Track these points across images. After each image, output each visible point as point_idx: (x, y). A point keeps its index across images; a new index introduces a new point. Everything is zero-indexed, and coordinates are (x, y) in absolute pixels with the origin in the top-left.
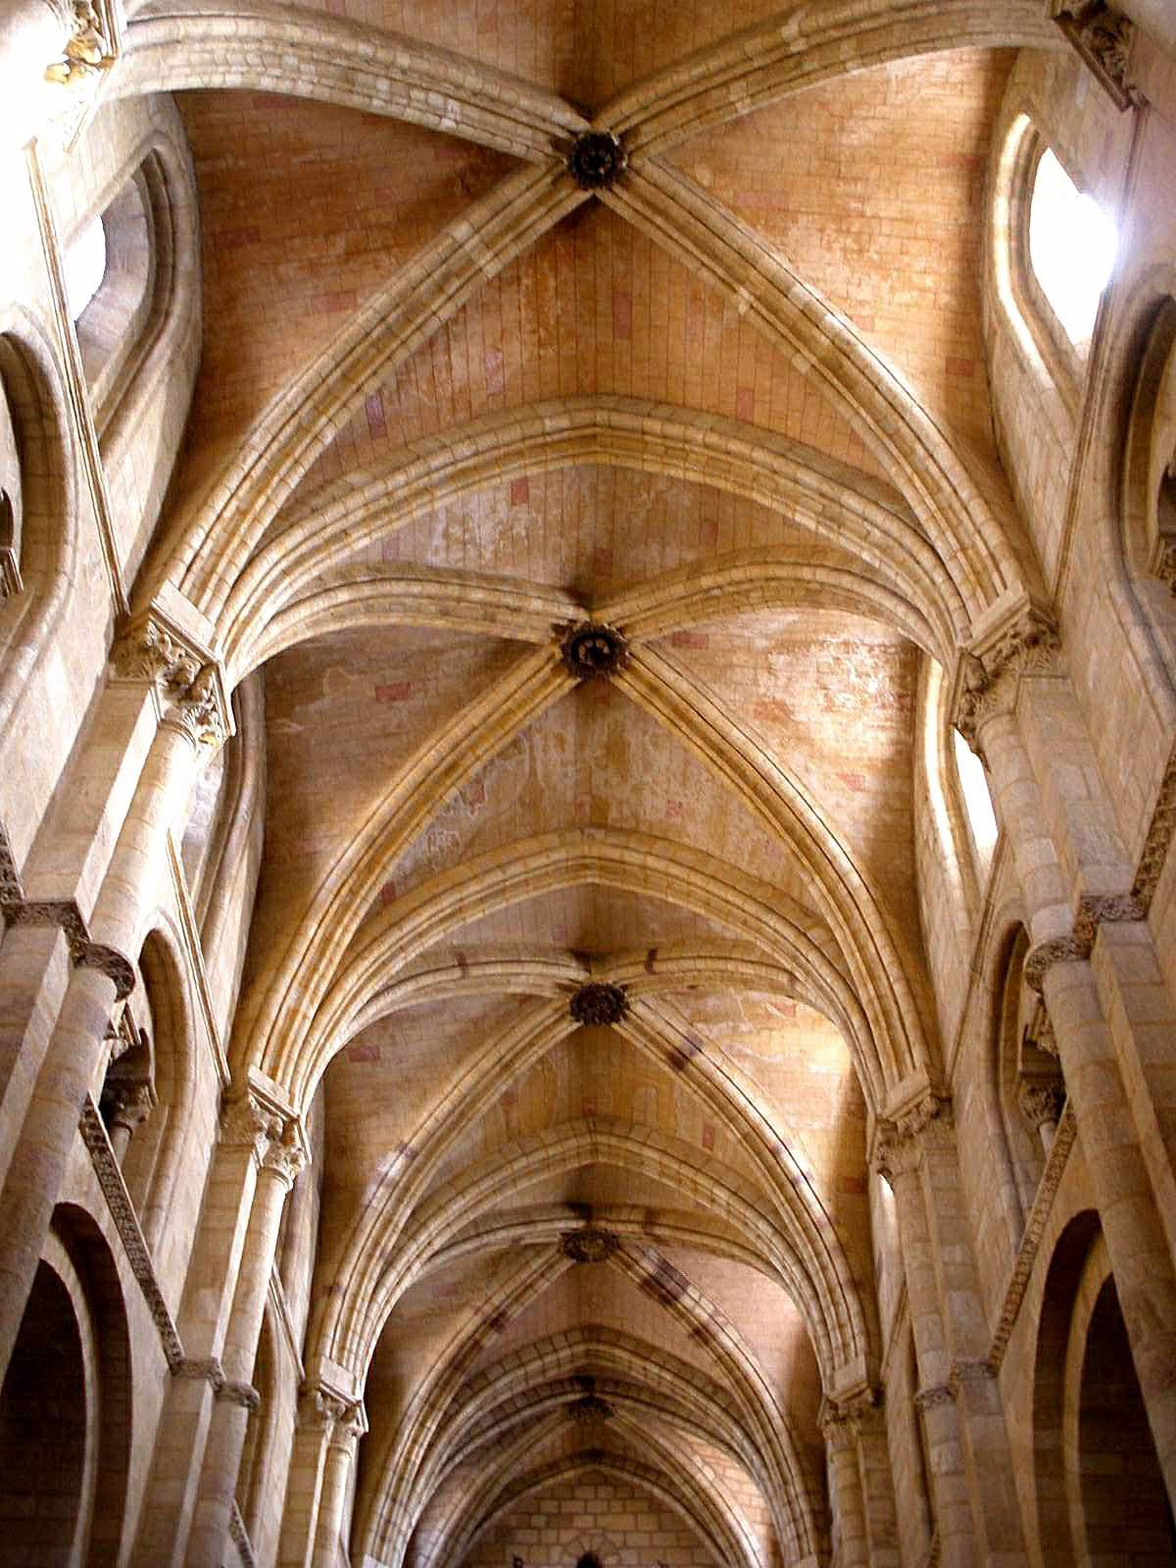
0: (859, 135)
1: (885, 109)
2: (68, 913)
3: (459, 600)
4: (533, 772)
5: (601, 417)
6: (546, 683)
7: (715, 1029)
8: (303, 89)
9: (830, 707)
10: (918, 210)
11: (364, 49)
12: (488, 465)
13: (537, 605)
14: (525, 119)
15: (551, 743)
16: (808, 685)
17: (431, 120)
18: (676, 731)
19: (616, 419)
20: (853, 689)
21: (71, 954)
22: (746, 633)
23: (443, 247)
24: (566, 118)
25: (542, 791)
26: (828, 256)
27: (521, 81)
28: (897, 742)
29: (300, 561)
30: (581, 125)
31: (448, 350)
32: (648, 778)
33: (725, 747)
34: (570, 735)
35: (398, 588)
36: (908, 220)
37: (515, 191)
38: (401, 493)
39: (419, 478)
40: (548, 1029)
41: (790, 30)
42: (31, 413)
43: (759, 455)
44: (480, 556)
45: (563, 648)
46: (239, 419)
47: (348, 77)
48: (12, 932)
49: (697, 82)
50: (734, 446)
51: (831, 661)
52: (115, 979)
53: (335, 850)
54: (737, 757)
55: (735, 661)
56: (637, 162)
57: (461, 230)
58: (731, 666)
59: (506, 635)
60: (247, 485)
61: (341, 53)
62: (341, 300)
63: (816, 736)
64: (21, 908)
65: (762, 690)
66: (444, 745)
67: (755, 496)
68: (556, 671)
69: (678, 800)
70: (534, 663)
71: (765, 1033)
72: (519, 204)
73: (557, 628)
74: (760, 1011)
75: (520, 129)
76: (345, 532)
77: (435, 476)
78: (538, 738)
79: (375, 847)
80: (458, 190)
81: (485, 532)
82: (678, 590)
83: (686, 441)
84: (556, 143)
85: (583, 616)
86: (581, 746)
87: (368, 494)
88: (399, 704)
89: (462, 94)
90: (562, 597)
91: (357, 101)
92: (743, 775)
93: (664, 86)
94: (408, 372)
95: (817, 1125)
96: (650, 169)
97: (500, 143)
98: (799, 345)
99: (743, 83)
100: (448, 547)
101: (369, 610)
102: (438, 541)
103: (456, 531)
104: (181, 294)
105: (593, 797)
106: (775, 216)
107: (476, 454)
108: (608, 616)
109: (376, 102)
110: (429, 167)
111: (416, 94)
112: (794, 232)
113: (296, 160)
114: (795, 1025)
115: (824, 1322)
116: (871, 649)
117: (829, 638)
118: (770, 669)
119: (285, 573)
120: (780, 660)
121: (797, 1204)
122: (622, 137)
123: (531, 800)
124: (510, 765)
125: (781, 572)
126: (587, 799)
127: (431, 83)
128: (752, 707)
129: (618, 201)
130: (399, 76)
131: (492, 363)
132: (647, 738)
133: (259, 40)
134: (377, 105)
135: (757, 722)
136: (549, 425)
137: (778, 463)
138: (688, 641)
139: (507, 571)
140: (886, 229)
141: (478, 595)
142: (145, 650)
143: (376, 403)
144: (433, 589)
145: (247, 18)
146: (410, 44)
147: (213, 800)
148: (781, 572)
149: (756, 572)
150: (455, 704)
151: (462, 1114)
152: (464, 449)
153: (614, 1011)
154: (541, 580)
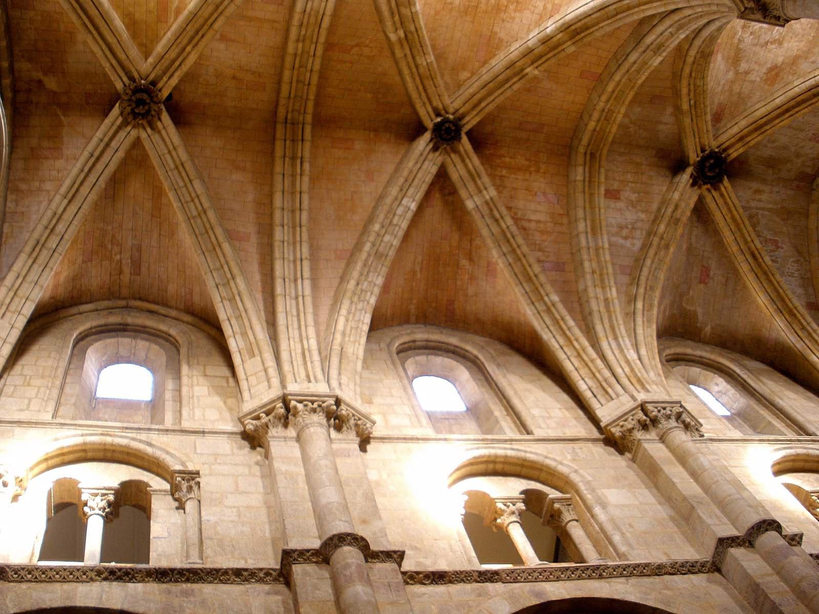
2: (724, 543)
3: (662, 238)
4: (770, 210)
5: (582, 150)
6: (722, 195)
8: (380, 281)
11: (367, 247)
12: (593, 214)
13: (676, 196)
14: (419, 165)
15: (758, 197)
16: (762, 53)
17: (410, 215)
18: (768, 132)
19: (585, 141)
21: (746, 547)
23: (477, 217)
24: (423, 143)
25: (783, 207)
26: (517, 20)
27: (401, 162)
29: (613, 328)
30: (427, 136)
31: (529, 221)
32: (793, 149)
33: (784, 107)
34: (755, 185)
35: (645, 271)
37: (457, 172)
38: (594, 265)
39: (589, 254)
41: (393, 37)
42: (491, 466)
43: (617, 78)
44: (642, 221)
45: (705, 183)
46: (535, 338)
47: (379, 256)
48: (724, 570)
49: (414, 79)
50: (610, 88)
51: (751, 37)
52: (767, 530)
53: (778, 330)
54: (793, 103)
55: (738, 91)
56: (451, 110)
57: (470, 204)
58: (739, 94)
59: (688, 213)
60: (566, 349)
61: (366, 260)
62: (491, 270)
63: (795, 53)
64: (714, 563)
65: (758, 79)
66: (740, 258)
67: (640, 82)
69: (810, 135)
70: (709, 199)
72: (463, 172)
73: (693, 185)
75: (424, 167)
76: (606, 300)
77: (591, 244)
78: (753, 204)
79: (782, 310)
80: (451, 198)
81: (630, 216)
82: (687, 121)
83: (603, 110)
84: (435, 149)
85: (689, 170)
86: (764, 181)
87: (589, 283)
88: (711, 274)
89: (400, 197)
90: (677, 179)
91: (392, 253)
92: (804, 101)
93: (414, 95)
94: (535, 244)
96: (456, 105)
97: (429, 179)
98: (560, 49)
99: (418, 58)
100: (633, 238)
101: (652, 288)
102: (628, 243)
103: (625, 232)
104: (468, 347)
105: (795, 180)
106: (492, 44)
107: (585, 220)
108: (693, 156)
109: (395, 243)
110: (436, 212)
111: (395, 221)
112: (502, 35)
113: (419, 276)
117: (738, 37)
119: (616, 338)
120: (744, 66)
122: (438, 115)
123: (786, 214)
124: (763, 222)
125: (687, 70)
126: (795, 183)
127: (391, 212)
128: (766, 87)
129: (470, 122)
130: (384, 230)
131: (542, 198)
132: (769, 145)
133: (352, 302)
134: (396, 243)
135: (776, 86)
136: (580, 178)
137: (623, 69)
138: (720, 115)
139: (655, 206)
141: (662, 227)
142: (623, 437)
143: (547, 265)
144: (652, 252)
145: (340, 308)
146: (370, 220)
147: (729, 387)
148: (687, 70)
149: (684, 82)
150: (719, 244)
152: (581, 226)
154: (665, 188)
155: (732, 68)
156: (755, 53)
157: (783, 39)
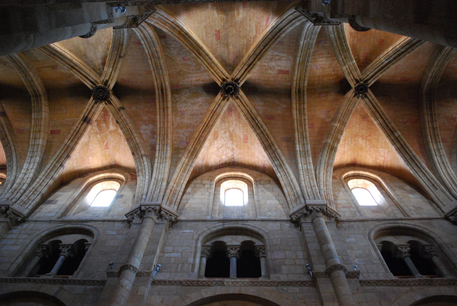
0: (361, 142)
1: (369, 147)
4: (190, 73)
7: (96, 128)
9: (218, 148)
10: (346, 155)
15: (198, 78)
20: (223, 153)
22: (234, 125)
28: (212, 166)
32: (189, 104)
36: (344, 154)
40: (87, 78)
56: (360, 98)
58: (225, 123)
65: (220, 131)
68: (224, 80)
69: (186, 114)
71: (98, 142)
74: (104, 139)
86: (196, 86)
88: (215, 37)
95: (75, 164)
114: (102, 150)
115: (25, 191)
116: (232, 155)
118: (225, 132)
120: (227, 134)
121: (54, 168)
132: (201, 103)
140: (343, 149)
151: (55, 55)
153: (98, 99)
155: (232, 132)
156: (225, 141)
157: (217, 151)
